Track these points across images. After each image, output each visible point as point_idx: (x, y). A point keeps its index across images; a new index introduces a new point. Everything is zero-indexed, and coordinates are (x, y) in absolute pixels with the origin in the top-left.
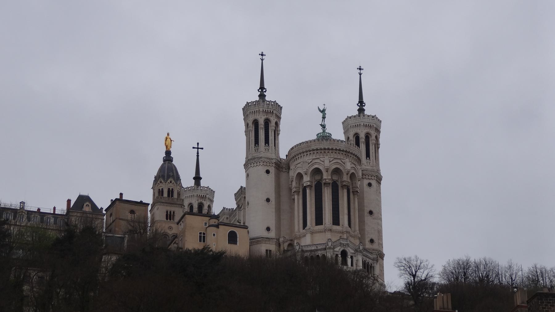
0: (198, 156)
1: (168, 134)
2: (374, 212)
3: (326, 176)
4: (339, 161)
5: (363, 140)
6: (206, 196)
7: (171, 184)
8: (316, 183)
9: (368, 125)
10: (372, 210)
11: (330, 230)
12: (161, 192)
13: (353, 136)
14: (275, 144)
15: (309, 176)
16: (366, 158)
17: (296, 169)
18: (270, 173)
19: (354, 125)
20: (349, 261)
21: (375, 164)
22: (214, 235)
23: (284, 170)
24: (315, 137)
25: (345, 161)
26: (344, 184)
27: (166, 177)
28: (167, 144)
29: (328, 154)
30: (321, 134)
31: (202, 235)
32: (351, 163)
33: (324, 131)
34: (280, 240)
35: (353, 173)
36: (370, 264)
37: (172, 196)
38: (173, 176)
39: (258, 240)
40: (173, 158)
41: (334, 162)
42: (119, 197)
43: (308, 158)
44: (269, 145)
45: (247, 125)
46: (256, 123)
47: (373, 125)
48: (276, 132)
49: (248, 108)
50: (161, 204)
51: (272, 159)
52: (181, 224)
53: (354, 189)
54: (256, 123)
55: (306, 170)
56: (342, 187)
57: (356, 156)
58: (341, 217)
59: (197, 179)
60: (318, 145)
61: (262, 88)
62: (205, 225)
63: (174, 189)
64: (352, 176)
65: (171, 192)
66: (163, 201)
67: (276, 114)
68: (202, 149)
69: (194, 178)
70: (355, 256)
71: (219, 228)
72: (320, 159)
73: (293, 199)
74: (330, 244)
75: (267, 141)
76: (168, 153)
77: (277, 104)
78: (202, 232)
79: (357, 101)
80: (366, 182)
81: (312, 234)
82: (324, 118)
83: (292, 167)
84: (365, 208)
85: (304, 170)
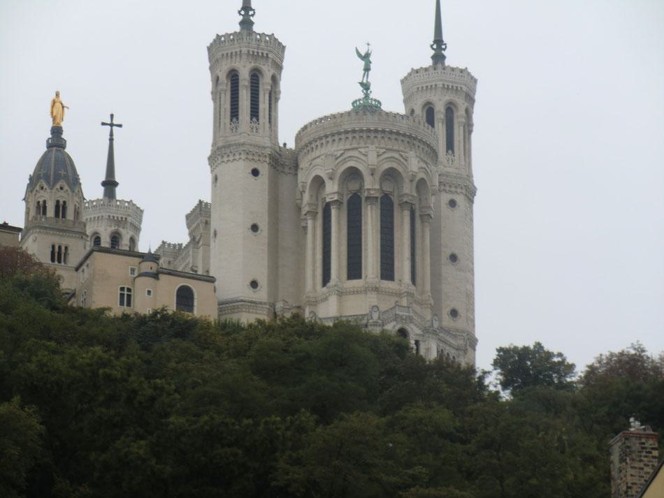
0: (111, 140)
1: (57, 95)
2: (459, 256)
3: (371, 185)
4: (396, 155)
5: (442, 116)
6: (126, 219)
7: (62, 193)
8: (349, 196)
9: (452, 87)
10: (456, 252)
11: (376, 289)
12: (41, 208)
13: (420, 109)
14: (270, 118)
16: (447, 152)
17: (312, 168)
18: (260, 176)
19: (424, 85)
21: (463, 163)
22: (149, 292)
23: (287, 170)
24: (349, 108)
26: (405, 199)
27: (52, 177)
28: (54, 114)
29: (375, 140)
30: (361, 102)
31: (126, 293)
32: (419, 159)
33: (367, 96)
34: (277, 307)
35: (422, 179)
37: (64, 216)
38: (66, 178)
39: (234, 304)
40: (65, 141)
41: (386, 156)
43: (336, 148)
44: (258, 120)
45: (216, 81)
46: (233, 76)
47: (461, 88)
48: (274, 96)
49: (218, 46)
50: (42, 231)
51: (265, 148)
52: (83, 271)
53: (423, 210)
54: (233, 76)
55: (331, 171)
56: (400, 204)
57: (429, 146)
58: (396, 264)
59: (110, 184)
60: (356, 122)
62: (131, 274)
63: (67, 203)
64: (421, 185)
65: (60, 209)
68: (120, 126)
69: (104, 184)
70: (424, 341)
71: (158, 279)
72: (360, 150)
73: (303, 227)
74: (375, 316)
75: (255, 112)
76: (57, 131)
77: (276, 40)
78: (126, 287)
79: (431, 38)
80: (445, 198)
82: (367, 69)
83: (303, 164)
85: (327, 172)
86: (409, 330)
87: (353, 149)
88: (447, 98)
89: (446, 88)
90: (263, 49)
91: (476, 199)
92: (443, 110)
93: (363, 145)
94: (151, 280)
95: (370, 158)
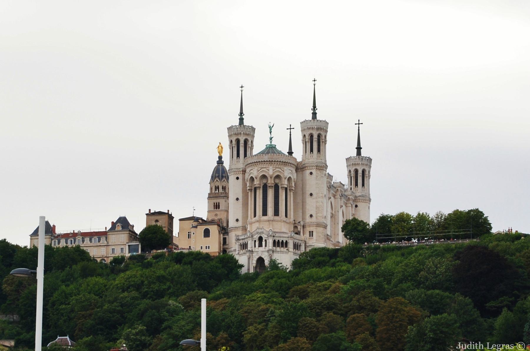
0: (290, 135)
7: (217, 183)
13: (308, 135)
20: (264, 243)
22: (194, 233)
25: (269, 168)
33: (271, 143)
36: (285, 241)
40: (223, 161)
42: (148, 212)
51: (240, 169)
61: (241, 113)
66: (212, 196)
67: (244, 134)
70: (268, 239)
76: (220, 158)
81: (251, 224)
84: (307, 192)
86: (262, 236)
90: (239, 131)
94: (194, 229)
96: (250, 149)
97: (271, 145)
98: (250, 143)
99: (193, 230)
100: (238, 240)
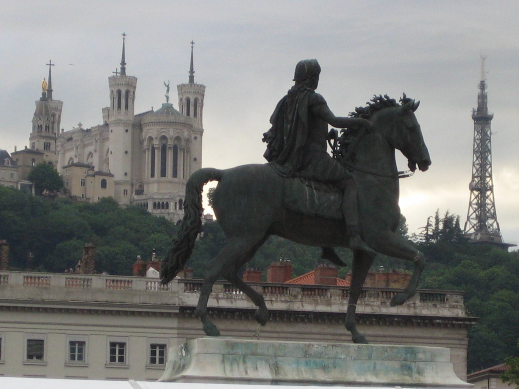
0: (50, 71)
2: (198, 158)
3: (170, 143)
4: (180, 131)
5: (193, 104)
11: (170, 182)
12: (40, 127)
15: (158, 140)
22: (92, 182)
26: (182, 147)
31: (83, 181)
33: (168, 101)
35: (188, 139)
37: (48, 131)
45: (112, 92)
47: (200, 92)
54: (119, 92)
68: (53, 65)
75: (127, 107)
78: (83, 179)
80: (193, 137)
82: (168, 91)
83: (145, 129)
87: (165, 128)
88: (195, 96)
89: (195, 93)
91: (204, 134)
92: (193, 101)
93: (168, 127)
95: (171, 133)
96: (131, 101)
97: (168, 104)
98: (131, 94)
99: (89, 180)
100: (154, 199)
